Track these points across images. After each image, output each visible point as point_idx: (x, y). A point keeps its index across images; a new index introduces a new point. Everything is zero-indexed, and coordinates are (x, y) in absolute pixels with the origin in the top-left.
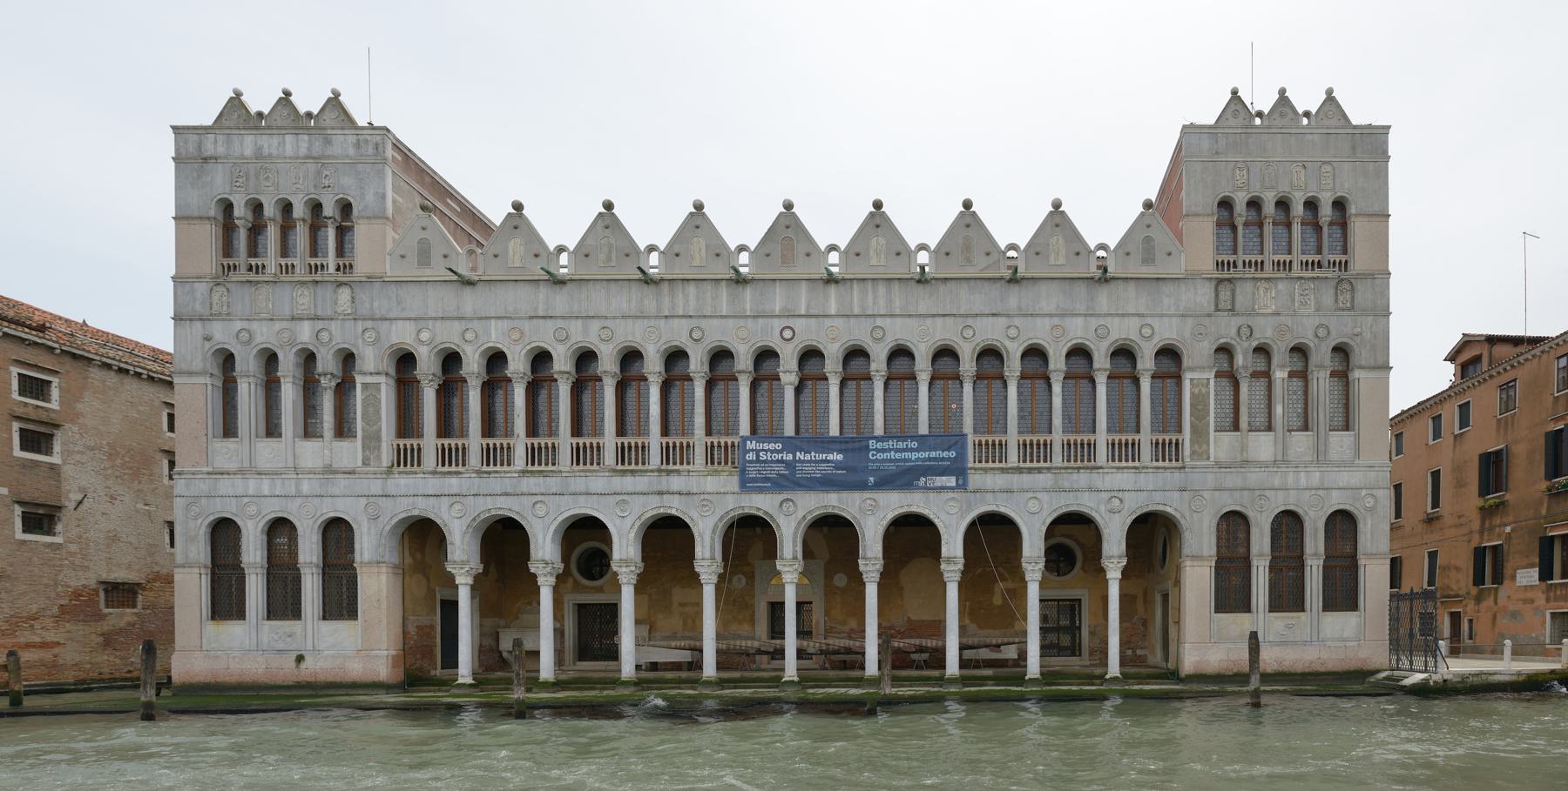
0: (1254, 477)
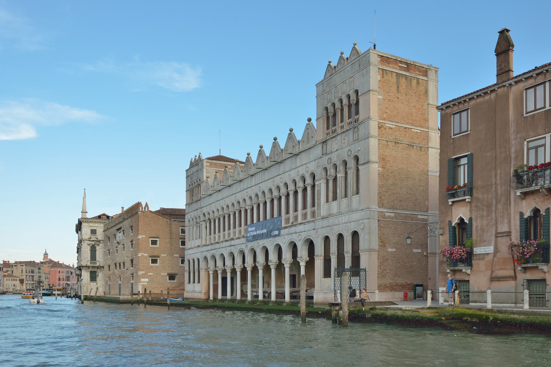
0: (331, 221)
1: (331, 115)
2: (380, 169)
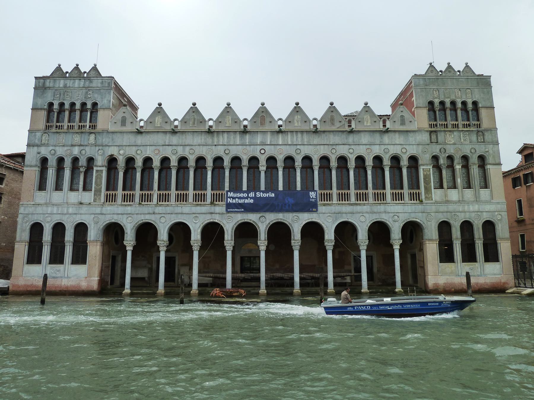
0: (451, 207)
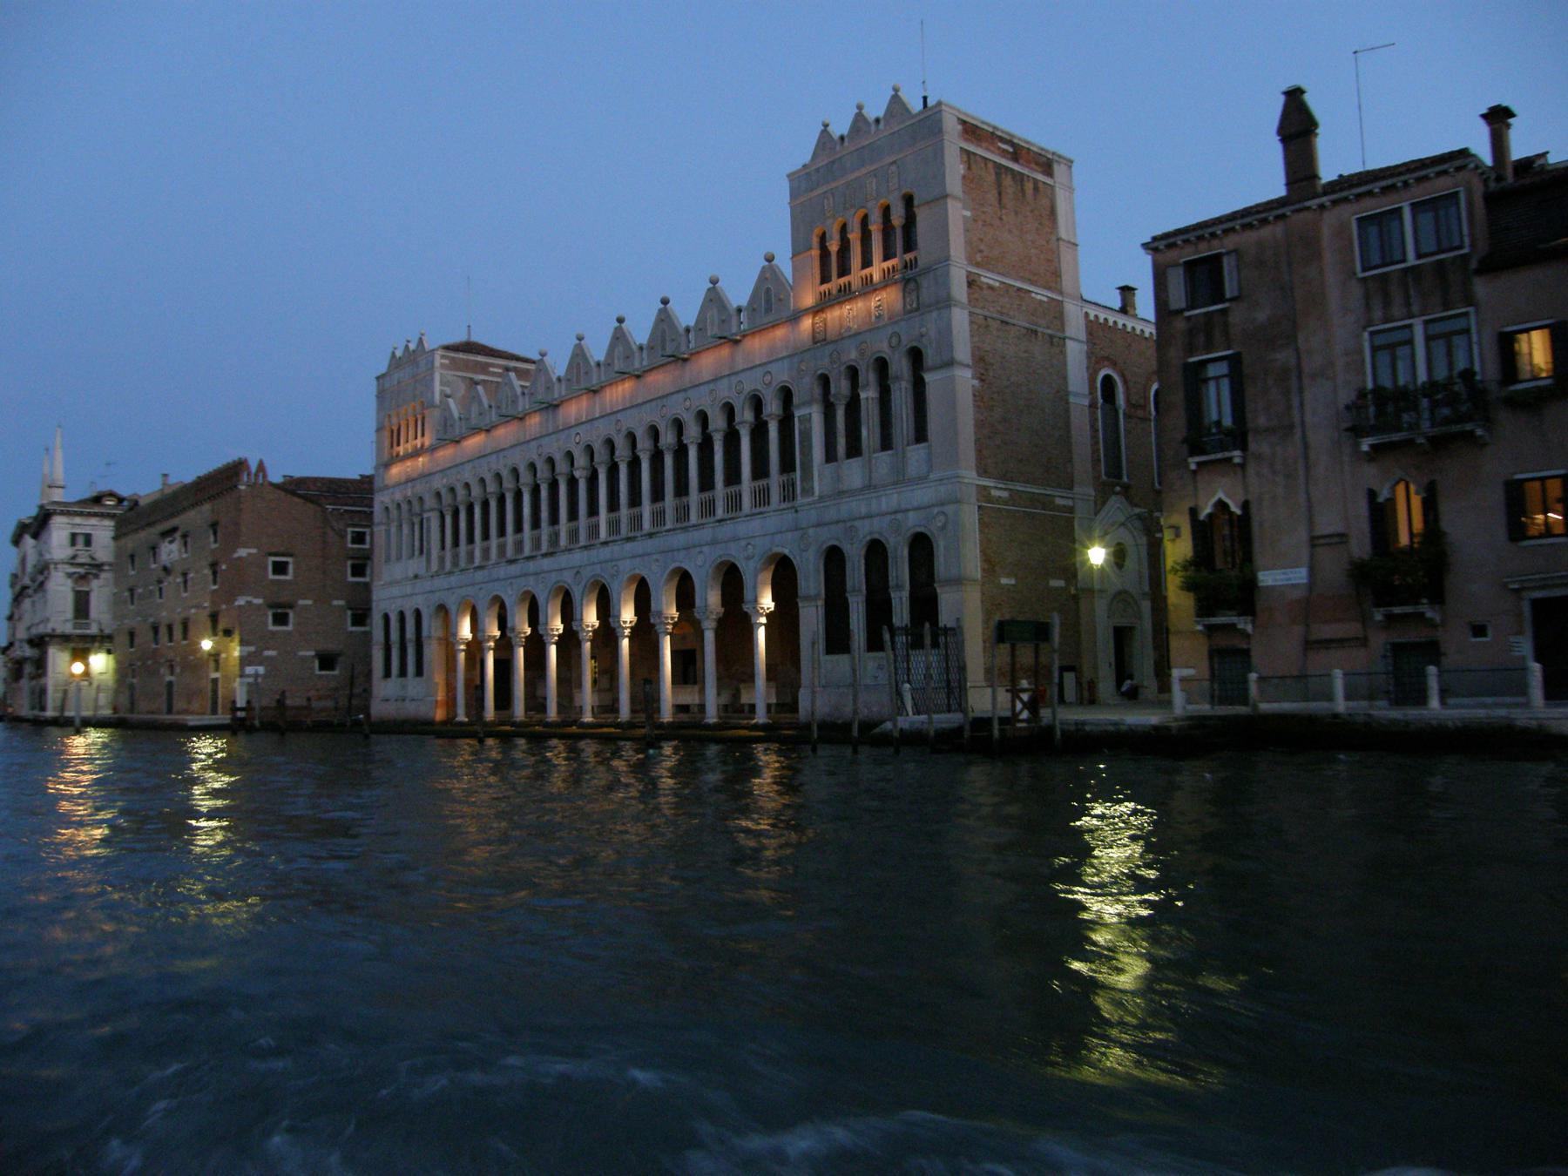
1: (834, 247)
2: (976, 382)
